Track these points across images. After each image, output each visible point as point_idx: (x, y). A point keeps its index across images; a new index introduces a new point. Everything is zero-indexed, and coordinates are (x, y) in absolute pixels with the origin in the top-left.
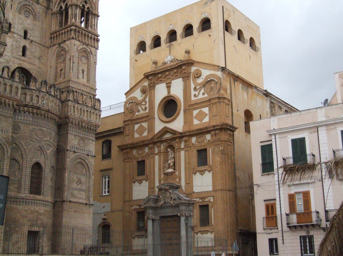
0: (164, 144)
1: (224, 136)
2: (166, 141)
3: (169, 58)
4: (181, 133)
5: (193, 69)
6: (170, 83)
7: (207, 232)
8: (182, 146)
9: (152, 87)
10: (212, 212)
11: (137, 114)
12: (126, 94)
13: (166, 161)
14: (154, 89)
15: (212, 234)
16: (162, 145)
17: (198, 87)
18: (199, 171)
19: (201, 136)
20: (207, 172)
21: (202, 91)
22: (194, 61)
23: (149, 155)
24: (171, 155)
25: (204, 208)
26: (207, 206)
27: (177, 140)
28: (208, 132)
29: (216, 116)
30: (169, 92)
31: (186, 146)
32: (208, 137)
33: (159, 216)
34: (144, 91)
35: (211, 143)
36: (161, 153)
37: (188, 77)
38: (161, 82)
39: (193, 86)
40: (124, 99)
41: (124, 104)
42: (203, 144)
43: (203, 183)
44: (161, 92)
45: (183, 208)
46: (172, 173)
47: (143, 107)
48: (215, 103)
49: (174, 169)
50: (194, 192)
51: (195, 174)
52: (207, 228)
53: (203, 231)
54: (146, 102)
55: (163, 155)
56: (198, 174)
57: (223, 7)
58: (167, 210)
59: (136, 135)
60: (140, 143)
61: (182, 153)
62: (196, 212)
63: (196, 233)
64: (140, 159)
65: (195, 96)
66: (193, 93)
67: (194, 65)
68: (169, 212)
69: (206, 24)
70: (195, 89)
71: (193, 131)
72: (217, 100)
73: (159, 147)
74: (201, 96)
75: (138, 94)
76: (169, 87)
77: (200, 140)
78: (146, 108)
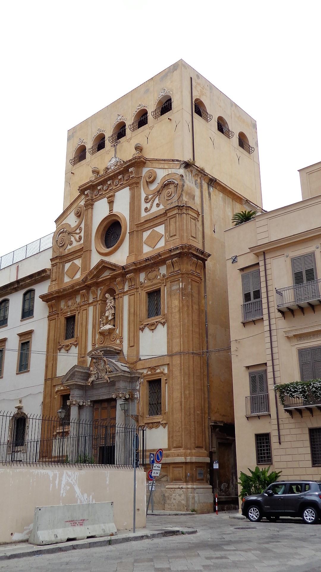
0: (102, 288)
1: (187, 266)
3: (114, 161)
4: (123, 268)
5: (145, 171)
6: (113, 196)
7: (157, 424)
8: (126, 288)
9: (90, 205)
10: (165, 389)
11: (69, 247)
12: (56, 221)
13: (103, 312)
14: (92, 208)
15: (164, 427)
16: (99, 289)
17: (150, 197)
18: (148, 324)
19: (153, 270)
20: (160, 326)
21: (157, 201)
22: (146, 160)
23: (80, 307)
24: (110, 303)
25: (155, 384)
26: (159, 381)
27: (119, 279)
28: (163, 262)
29: (175, 235)
30: (111, 210)
32: (163, 270)
34: (79, 215)
35: (167, 278)
36: (97, 301)
37: (137, 183)
38: (102, 197)
39: (143, 196)
40: (53, 228)
41: (53, 235)
42: (155, 281)
43: (154, 344)
44: (101, 211)
45: (121, 385)
46: (110, 331)
47: (77, 237)
48: (174, 216)
49: (114, 326)
50: (140, 360)
51: (142, 331)
52: (158, 418)
53: (152, 423)
54: (81, 229)
56: (147, 330)
57: (191, 78)
59: (67, 279)
60: (69, 289)
61: (126, 298)
62: (142, 392)
64: (69, 314)
66: (144, 205)
68: (103, 394)
69: (166, 106)
70: (147, 200)
71: (140, 263)
72: (176, 212)
73: (94, 293)
74: (155, 209)
75: (72, 220)
76: (111, 203)
77: (152, 275)
78: (80, 238)
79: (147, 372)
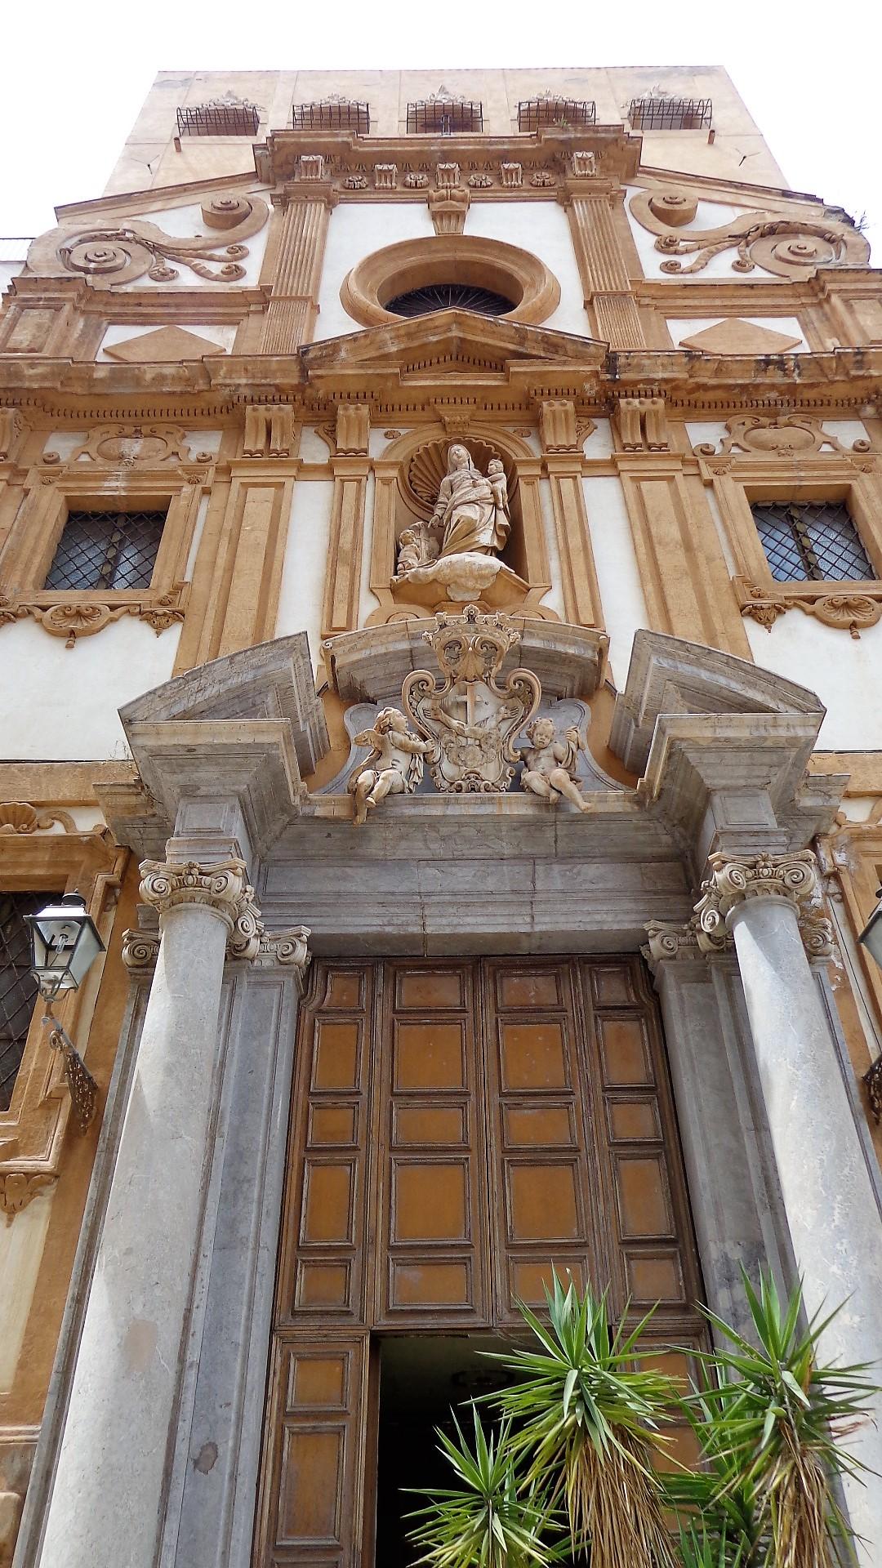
0: (403, 432)
2: (427, 406)
18: (812, 600)
33: (306, 932)
47: (216, 268)
51: (767, 623)
55: (386, 482)
58: (429, 878)
65: (670, 268)
67: (635, 181)
77: (767, 434)
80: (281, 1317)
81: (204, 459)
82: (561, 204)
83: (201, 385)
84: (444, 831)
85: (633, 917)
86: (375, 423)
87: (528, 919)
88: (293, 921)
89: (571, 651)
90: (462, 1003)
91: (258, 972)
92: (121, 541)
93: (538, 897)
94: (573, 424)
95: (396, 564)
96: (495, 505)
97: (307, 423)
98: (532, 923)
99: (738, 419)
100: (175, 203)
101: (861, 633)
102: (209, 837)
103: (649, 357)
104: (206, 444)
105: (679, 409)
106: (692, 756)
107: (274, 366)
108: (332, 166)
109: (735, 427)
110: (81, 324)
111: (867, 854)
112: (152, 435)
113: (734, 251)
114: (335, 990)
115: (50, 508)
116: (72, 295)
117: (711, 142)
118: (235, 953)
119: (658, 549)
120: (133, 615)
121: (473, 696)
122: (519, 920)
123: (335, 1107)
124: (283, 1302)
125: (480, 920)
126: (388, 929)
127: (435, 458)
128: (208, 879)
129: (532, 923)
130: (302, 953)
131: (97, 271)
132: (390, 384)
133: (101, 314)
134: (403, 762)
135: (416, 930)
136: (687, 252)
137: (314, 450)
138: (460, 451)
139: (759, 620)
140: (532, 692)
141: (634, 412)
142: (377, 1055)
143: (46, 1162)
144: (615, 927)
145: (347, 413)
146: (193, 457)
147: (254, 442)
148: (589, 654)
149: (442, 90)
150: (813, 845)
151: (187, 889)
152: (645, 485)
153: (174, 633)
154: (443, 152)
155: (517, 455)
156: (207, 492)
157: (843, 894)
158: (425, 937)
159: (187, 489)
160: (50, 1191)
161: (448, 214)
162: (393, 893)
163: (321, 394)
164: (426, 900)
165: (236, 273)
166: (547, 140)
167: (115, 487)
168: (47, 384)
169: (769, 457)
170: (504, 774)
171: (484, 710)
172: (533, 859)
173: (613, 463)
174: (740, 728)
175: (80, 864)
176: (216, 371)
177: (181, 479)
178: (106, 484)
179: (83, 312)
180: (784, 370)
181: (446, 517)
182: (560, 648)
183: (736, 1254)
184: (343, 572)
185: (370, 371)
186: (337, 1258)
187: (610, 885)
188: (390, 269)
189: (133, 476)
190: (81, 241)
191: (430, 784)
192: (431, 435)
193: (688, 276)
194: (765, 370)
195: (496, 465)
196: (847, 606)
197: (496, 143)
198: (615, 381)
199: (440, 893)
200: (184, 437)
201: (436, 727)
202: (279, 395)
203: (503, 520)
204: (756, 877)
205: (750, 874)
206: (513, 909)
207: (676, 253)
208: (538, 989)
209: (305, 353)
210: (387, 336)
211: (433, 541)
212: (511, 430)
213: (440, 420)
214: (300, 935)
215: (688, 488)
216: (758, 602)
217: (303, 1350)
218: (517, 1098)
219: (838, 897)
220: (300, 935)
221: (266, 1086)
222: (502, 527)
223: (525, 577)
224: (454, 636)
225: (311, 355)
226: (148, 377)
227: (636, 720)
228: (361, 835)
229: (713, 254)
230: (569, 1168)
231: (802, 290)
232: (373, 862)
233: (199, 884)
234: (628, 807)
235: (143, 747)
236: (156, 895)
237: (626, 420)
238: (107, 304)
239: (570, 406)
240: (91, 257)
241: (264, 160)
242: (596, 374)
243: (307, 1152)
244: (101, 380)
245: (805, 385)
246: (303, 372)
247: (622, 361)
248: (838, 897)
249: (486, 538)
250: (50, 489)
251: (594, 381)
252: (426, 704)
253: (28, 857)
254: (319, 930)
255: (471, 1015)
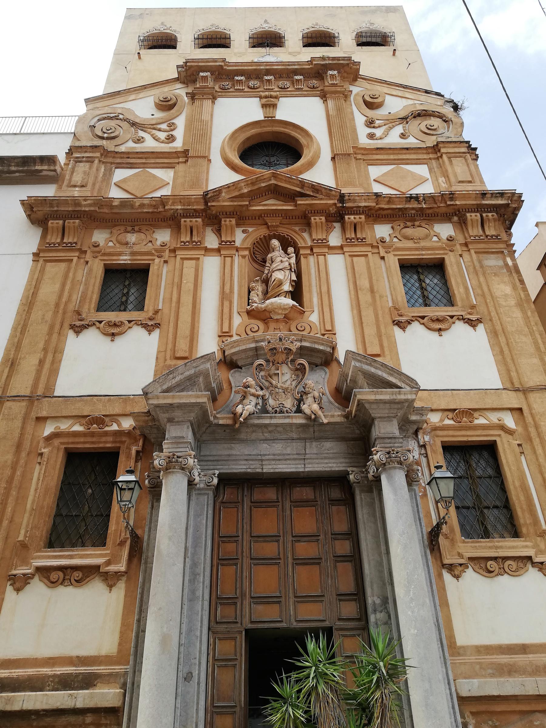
0: (250, 230)
2: (261, 218)
18: (423, 317)
26: (490, 449)
31: (349, 242)
33: (217, 472)
36: (237, 250)
47: (162, 136)
51: (403, 328)
55: (244, 257)
58: (264, 448)
63: (450, 568)
67: (357, 83)
77: (409, 231)
79: (442, 420)
80: (212, 624)
81: (163, 245)
82: (322, 99)
83: (161, 209)
84: (270, 429)
85: (344, 465)
86: (238, 225)
87: (303, 466)
88: (212, 467)
89: (321, 348)
90: (278, 498)
91: (199, 489)
92: (129, 284)
93: (307, 456)
94: (325, 228)
95: (249, 299)
96: (291, 269)
97: (208, 225)
98: (305, 468)
99: (398, 223)
100: (141, 95)
101: (443, 333)
102: (179, 438)
103: (358, 196)
104: (163, 236)
105: (371, 219)
106: (367, 406)
107: (193, 200)
108: (214, 77)
109: (395, 227)
110: (103, 169)
111: (437, 436)
112: (140, 231)
113: (401, 126)
114: (228, 494)
115: (98, 269)
116: (98, 155)
117: (394, 54)
118: (191, 483)
119: (359, 292)
120: (138, 325)
121: (281, 371)
122: (299, 466)
123: (229, 542)
124: (212, 618)
125: (284, 466)
126: (249, 470)
127: (264, 241)
128: (180, 460)
129: (305, 468)
130: (215, 481)
131: (108, 138)
132: (244, 208)
133: (112, 163)
134: (254, 400)
135: (259, 470)
136: (379, 127)
137: (211, 240)
138: (275, 243)
139: (400, 327)
140: (305, 369)
141: (351, 223)
142: (245, 521)
143: (122, 567)
144: (337, 469)
145: (226, 222)
146: (159, 243)
147: (185, 238)
148: (329, 349)
149: (266, 21)
150: (416, 433)
151: (173, 464)
152: (355, 259)
153: (156, 333)
154: (267, 69)
155: (301, 243)
156: (166, 262)
157: (427, 454)
158: (263, 473)
159: (157, 260)
160: (124, 578)
161: (269, 105)
162: (250, 455)
163: (214, 212)
164: (264, 458)
165: (171, 139)
166: (315, 64)
167: (125, 259)
168: (92, 209)
169: (409, 244)
170: (294, 404)
171: (286, 377)
172: (305, 439)
173: (341, 247)
174: (386, 395)
175: (125, 441)
176: (167, 202)
177: (154, 255)
178: (122, 258)
179: (103, 162)
180: (418, 201)
181: (269, 275)
182: (317, 346)
183: (378, 601)
184: (226, 304)
185: (236, 204)
186: (231, 602)
187: (335, 451)
188: (242, 137)
189: (133, 254)
190: (99, 120)
191: (264, 410)
192: (263, 232)
193: (379, 141)
194: (410, 201)
195: (291, 250)
196: (438, 320)
197: (292, 65)
198: (343, 207)
199: (269, 455)
200: (154, 232)
201: (267, 384)
202: (195, 214)
203: (294, 278)
204: (390, 457)
205: (387, 456)
206: (297, 462)
207: (374, 127)
208: (307, 493)
209: (207, 195)
210: (243, 184)
211: (264, 285)
212: (297, 229)
213: (266, 224)
214: (214, 474)
215: (374, 259)
216: (400, 319)
217: (221, 636)
218: (298, 538)
219: (425, 455)
220: (214, 474)
221: (204, 537)
222: (294, 281)
223: (303, 308)
224: (274, 347)
225: (209, 196)
226: (137, 204)
227: (347, 381)
228: (238, 431)
229: (391, 128)
230: (318, 566)
231: (430, 151)
232: (242, 441)
233: (177, 461)
234: (342, 419)
235: (152, 404)
236: (161, 467)
237: (348, 226)
238: (114, 157)
239: (323, 218)
240: (104, 130)
241: (182, 73)
242: (335, 204)
243: (220, 561)
244: (116, 206)
245: (427, 208)
246: (206, 203)
247: (347, 198)
248: (425, 455)
249: (287, 287)
250: (97, 260)
251: (334, 207)
252: (262, 373)
253: (104, 439)
254: (222, 471)
255: (280, 504)
